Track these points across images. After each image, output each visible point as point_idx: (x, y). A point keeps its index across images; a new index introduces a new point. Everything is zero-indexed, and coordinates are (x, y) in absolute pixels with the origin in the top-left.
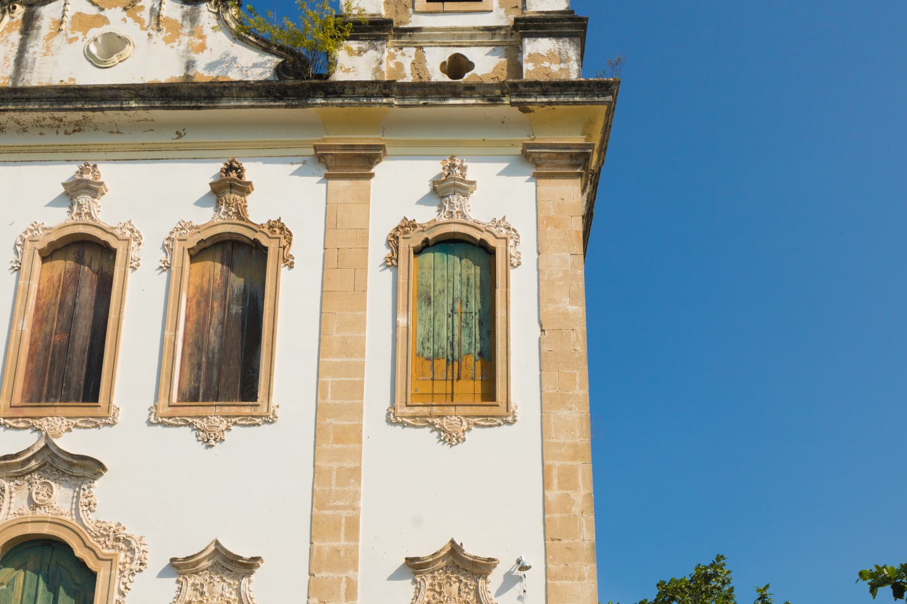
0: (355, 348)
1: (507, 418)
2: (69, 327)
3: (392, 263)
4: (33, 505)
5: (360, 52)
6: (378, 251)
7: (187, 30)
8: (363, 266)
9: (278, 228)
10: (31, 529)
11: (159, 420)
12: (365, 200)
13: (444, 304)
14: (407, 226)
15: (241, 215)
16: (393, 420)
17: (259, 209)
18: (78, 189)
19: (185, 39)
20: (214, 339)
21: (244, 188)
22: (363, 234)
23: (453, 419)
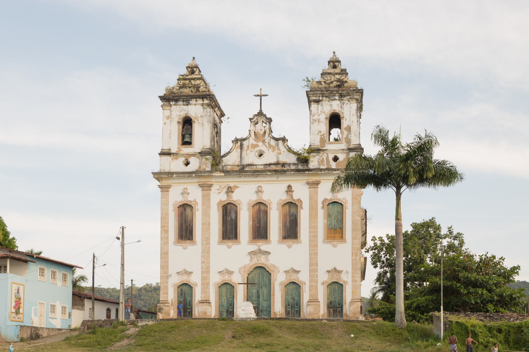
0: (316, 227)
1: (345, 241)
2: (259, 222)
3: (323, 207)
4: (258, 261)
5: (315, 156)
6: (320, 205)
7: (276, 148)
8: (316, 210)
9: (299, 200)
10: (258, 265)
11: (280, 242)
12: (317, 193)
13: (333, 217)
14: (326, 200)
15: (292, 197)
16: (324, 242)
17: (296, 196)
18: (259, 191)
19: (276, 151)
20: (288, 225)
21: (293, 191)
22: (317, 201)
23: (335, 243)
